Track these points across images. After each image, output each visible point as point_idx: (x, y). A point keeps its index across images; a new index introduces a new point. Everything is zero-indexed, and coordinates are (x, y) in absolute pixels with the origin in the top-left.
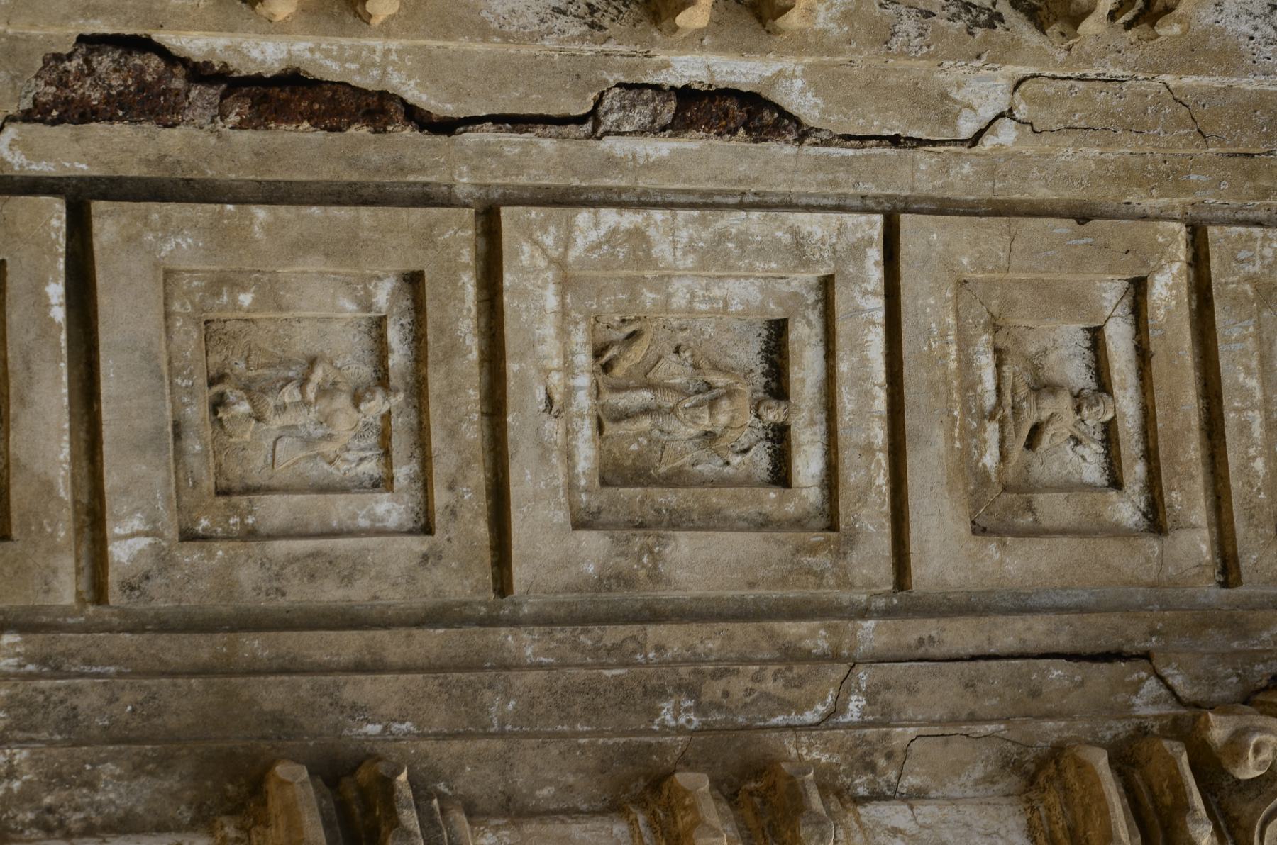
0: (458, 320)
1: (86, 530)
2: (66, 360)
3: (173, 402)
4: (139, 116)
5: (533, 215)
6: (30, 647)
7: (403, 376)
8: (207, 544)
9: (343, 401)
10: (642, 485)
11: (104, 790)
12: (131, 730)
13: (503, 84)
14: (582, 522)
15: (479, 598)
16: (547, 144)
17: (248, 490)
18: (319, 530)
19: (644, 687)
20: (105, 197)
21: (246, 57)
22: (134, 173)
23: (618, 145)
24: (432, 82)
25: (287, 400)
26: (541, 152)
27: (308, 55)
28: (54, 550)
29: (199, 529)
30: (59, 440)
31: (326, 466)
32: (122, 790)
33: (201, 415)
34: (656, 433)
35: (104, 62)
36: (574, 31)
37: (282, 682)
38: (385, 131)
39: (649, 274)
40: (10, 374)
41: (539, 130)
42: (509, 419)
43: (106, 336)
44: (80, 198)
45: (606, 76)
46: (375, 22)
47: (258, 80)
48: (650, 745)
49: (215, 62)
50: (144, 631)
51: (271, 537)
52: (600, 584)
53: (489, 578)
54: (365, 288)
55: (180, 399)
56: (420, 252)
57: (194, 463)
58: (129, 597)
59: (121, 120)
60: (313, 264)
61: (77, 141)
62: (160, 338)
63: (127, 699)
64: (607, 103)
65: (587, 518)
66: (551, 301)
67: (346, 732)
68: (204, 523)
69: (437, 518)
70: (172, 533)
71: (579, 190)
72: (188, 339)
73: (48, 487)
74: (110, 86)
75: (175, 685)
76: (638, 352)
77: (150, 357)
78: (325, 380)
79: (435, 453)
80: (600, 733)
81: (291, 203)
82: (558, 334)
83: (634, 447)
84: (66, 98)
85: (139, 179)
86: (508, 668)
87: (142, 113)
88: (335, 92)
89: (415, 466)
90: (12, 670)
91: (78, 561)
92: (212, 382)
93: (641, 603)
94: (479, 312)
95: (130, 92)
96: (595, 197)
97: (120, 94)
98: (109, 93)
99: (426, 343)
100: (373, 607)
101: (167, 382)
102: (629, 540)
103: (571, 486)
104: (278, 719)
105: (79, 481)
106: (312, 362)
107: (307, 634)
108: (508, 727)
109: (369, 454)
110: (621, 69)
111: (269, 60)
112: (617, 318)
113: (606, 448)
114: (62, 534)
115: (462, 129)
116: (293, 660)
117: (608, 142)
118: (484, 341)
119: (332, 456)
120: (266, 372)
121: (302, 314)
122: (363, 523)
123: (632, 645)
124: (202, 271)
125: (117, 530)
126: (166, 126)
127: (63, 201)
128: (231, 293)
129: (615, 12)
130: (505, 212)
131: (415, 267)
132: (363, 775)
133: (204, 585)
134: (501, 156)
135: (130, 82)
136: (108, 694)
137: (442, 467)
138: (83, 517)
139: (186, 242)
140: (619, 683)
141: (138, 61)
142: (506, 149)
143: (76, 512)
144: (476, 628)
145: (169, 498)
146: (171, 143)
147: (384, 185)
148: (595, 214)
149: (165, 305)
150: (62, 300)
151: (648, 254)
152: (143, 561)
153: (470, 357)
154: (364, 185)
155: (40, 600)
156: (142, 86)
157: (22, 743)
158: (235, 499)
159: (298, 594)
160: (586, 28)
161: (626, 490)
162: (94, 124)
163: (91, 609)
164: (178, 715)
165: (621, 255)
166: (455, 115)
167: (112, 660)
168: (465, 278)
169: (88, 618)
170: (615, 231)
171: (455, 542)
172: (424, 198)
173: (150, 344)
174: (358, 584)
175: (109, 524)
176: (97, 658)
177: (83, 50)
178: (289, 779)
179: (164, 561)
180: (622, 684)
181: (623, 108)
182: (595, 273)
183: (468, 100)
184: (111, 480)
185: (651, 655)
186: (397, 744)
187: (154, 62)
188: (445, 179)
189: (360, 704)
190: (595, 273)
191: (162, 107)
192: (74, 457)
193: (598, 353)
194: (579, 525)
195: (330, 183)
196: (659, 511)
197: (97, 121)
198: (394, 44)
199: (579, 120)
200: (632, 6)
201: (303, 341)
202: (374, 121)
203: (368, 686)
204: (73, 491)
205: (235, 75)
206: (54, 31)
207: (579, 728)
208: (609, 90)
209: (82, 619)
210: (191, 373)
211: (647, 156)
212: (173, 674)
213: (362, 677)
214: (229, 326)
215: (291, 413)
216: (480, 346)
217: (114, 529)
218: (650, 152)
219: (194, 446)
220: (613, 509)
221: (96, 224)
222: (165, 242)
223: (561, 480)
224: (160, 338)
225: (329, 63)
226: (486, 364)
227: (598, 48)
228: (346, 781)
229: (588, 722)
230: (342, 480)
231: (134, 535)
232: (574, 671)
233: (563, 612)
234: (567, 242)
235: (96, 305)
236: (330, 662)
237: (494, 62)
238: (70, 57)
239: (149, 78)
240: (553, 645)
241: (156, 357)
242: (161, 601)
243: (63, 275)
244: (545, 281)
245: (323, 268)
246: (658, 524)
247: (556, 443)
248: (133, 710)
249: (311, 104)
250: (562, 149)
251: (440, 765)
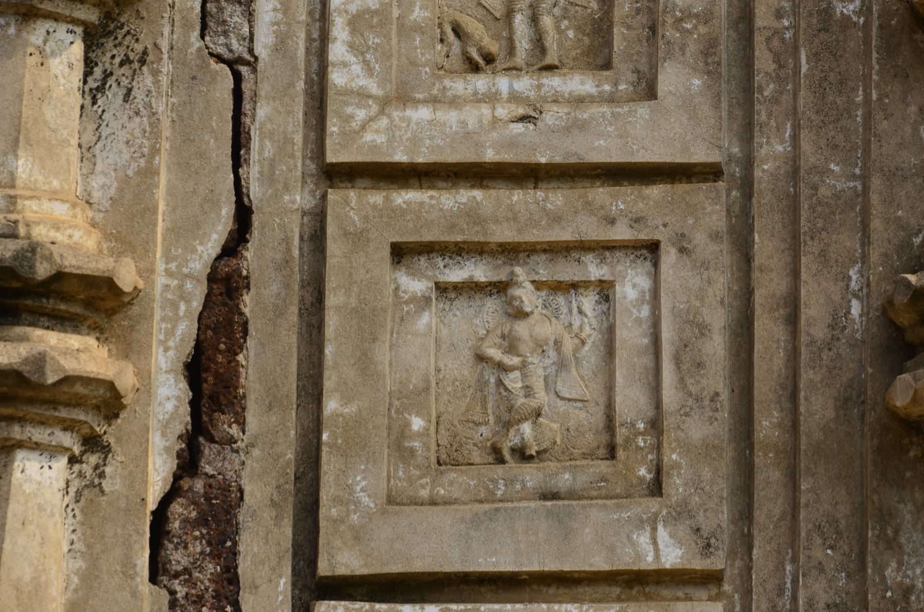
0: (441, 210)
1: (647, 590)
2: (478, 605)
3: (521, 500)
4: (232, 524)
5: (335, 129)
7: (497, 267)
8: (665, 469)
9: (522, 329)
10: (611, 26)
11: (912, 579)
12: (851, 551)
13: (202, 155)
14: (648, 90)
15: (724, 198)
16: (263, 111)
17: (610, 425)
18: (652, 357)
19: (820, 31)
20: (313, 562)
21: (173, 416)
22: (289, 531)
23: (263, 39)
24: (199, 228)
25: (520, 385)
26: (270, 119)
27: (171, 353)
29: (649, 477)
31: (587, 348)
32: (913, 561)
33: (535, 472)
34: (556, 11)
35: (177, 558)
36: (149, 81)
37: (806, 399)
38: (247, 277)
39: (396, 13)
41: (247, 121)
42: (543, 160)
43: (454, 564)
45: (193, 50)
46: (141, 285)
47: (195, 405)
48: (881, 27)
49: (177, 447)
50: (750, 536)
51: (658, 404)
52: (712, 73)
53: (704, 186)
54: (407, 303)
55: (517, 492)
56: (372, 246)
57: (582, 480)
58: (717, 549)
59: (235, 544)
60: (382, 354)
61: (256, 588)
62: (457, 510)
63: (818, 553)
64: (220, 50)
65: (644, 85)
66: (423, 113)
67: (858, 336)
68: (643, 472)
69: (643, 236)
70: (654, 504)
71: (309, 81)
72: (456, 482)
74: (202, 553)
75: (807, 506)
76: (474, 27)
77: (476, 522)
78: (500, 347)
79: (576, 237)
80: (867, 77)
81: (320, 375)
82: (456, 108)
83: (571, 33)
84: (213, 597)
85: (295, 527)
86: (796, 170)
87: (229, 522)
88: (208, 327)
89: (589, 258)
91: (678, 599)
92: (501, 460)
93: (731, 32)
94: (432, 187)
95: (208, 533)
96: (315, 66)
97: (209, 543)
98: (209, 555)
99: (464, 242)
100: (730, 305)
101: (500, 505)
102: (668, 42)
103: (611, 100)
104: (844, 403)
105: (598, 596)
106: (481, 358)
107: (757, 373)
108: (857, 171)
109: (574, 305)
110: (186, 35)
111: (177, 393)
112: (439, 47)
113: (571, 63)
115: (246, 199)
116: (782, 386)
117: (259, 50)
118: (462, 184)
119: (576, 341)
120: (490, 405)
121: (433, 367)
122: (645, 311)
123: (776, 43)
124: (389, 467)
125: (650, 559)
126: (242, 498)
127: (318, 603)
128: (411, 438)
129: (128, 37)
130: (331, 158)
131: (387, 251)
132: (904, 320)
133: (707, 473)
134: (274, 160)
135: (197, 533)
136: (815, 572)
137: (593, 231)
138: (634, 592)
139: (360, 482)
140: (815, 57)
141: (177, 524)
142: (266, 154)
143: (629, 599)
144: (754, 201)
145: (618, 506)
146: (259, 495)
147: (302, 280)
148: (334, 65)
149: (422, 504)
151: (375, 13)
152: (681, 534)
153: (479, 199)
154: (302, 300)
156: (202, 521)
158: (619, 440)
159: (717, 379)
160: (145, 68)
161: (615, 44)
162: (240, 571)
163: (727, 587)
164: (837, 503)
165: (376, 40)
166: (233, 206)
167: (780, 568)
168: (399, 201)
169: (736, 590)
170: (352, 46)
171: (667, 219)
172: (316, 239)
173: (462, 520)
174: (708, 319)
175: (643, 566)
176: (777, 582)
177: (164, 579)
178: (911, 393)
179: (681, 513)
180: (816, 54)
181: (225, 33)
182: (394, 68)
183: (217, 192)
184: (600, 563)
185: (786, 23)
186: (873, 284)
187: (177, 508)
188: (297, 218)
189: (830, 321)
190: (394, 68)
191: (224, 502)
193: (475, 68)
194: (651, 93)
195: (300, 334)
196: (638, 11)
197: (236, 567)
198: (160, 266)
199: (238, 78)
200: (122, 20)
201: (459, 368)
202: (237, 289)
203: (813, 312)
204: (608, 602)
205: (189, 427)
207: (859, 99)
208: (207, 48)
209: (736, 596)
210: (493, 481)
211: (275, 10)
212: (795, 507)
213: (803, 317)
214: (444, 442)
215: (532, 381)
216: (466, 188)
217: (648, 562)
218: (271, 6)
219: (564, 481)
220: (635, 57)
221: (342, 571)
222: (360, 502)
223: (606, 109)
224: (457, 510)
225: (179, 332)
226: (485, 183)
227: (166, 56)
228: (909, 337)
229: (854, 90)
230: (601, 331)
232: (801, 102)
233: (738, 113)
234: (363, 95)
235: (423, 573)
236: (785, 350)
237: (179, 164)
238: (172, 593)
239: (194, 514)
240: (773, 123)
241: (476, 514)
242: (719, 517)
243: (393, 605)
244: (402, 119)
245: (387, 345)
246: (651, 12)
247: (568, 114)
248: (831, 548)
249: (220, 352)
250: (266, 97)
251: (895, 241)
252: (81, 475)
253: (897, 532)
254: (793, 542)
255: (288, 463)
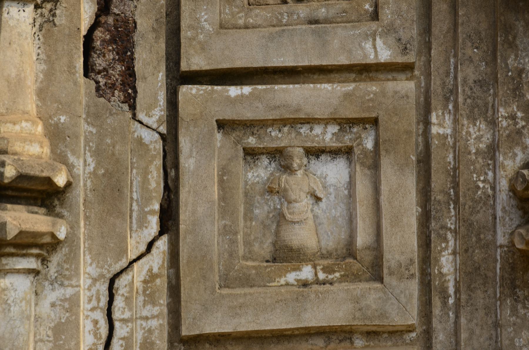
1: (371, 75)
2: (273, 86)
3: (297, 24)
4: (130, 42)
6: (439, 107)
8: (380, 5)
11: (524, 65)
12: (488, 49)
20: (178, 63)
22: (163, 46)
28: (383, 93)
29: (371, 9)
30: (320, 89)
32: (524, 54)
33: (305, 8)
35: (100, 63)
40: (282, 117)
43: (258, 62)
44: (179, 78)
50: (430, 42)
55: (295, 20)
57: (332, 12)
58: (411, 50)
59: (133, 53)
61: (145, 78)
62: (260, 31)
63: (469, 52)
68: (367, 6)
70: (374, 25)
73: (347, 96)
75: (462, 24)
77: (271, 38)
84: (121, 84)
85: (167, 43)
87: (128, 41)
90: (452, 117)
91: (388, 80)
95: (117, 48)
97: (118, 54)
98: (117, 60)
101: (285, 28)
105: (342, 79)
114: (374, 88)
124: (220, 7)
125: (372, 57)
126: (135, 27)
127: (181, 87)
133: (404, 7)
135: (110, 48)
136: (467, 62)
138: (363, 77)
139: (204, 16)
141: (98, 43)
143: (360, 81)
145: (354, 27)
146: (145, 25)
149: (240, 28)
150: (239, 87)
152: (390, 42)
155: (412, 101)
156: (113, 41)
157: (495, 111)
162: (136, 69)
163: (417, 73)
164: (480, 22)
167: (447, 60)
169: (422, 74)
173: (263, 37)
175: (368, 61)
176: (446, 69)
179: (389, 30)
184: (343, 60)
187: (98, 34)
191: (125, 29)
192: (329, 82)
197: (134, 67)
204: (348, 82)
206: (83, 91)
209: (422, 77)
210: (280, 14)
212: (455, 25)
217: (371, 59)
221: (194, 68)
222: (204, 28)
224: (260, 31)
231: (375, 47)
235: (241, 68)
238: (97, 82)
239: (108, 37)
241: (271, 33)
242: (412, 32)
243: (224, 87)
248: (477, 48)
252: (42, 15)
253: (515, 38)
254: (455, 46)
255: (162, 6)
